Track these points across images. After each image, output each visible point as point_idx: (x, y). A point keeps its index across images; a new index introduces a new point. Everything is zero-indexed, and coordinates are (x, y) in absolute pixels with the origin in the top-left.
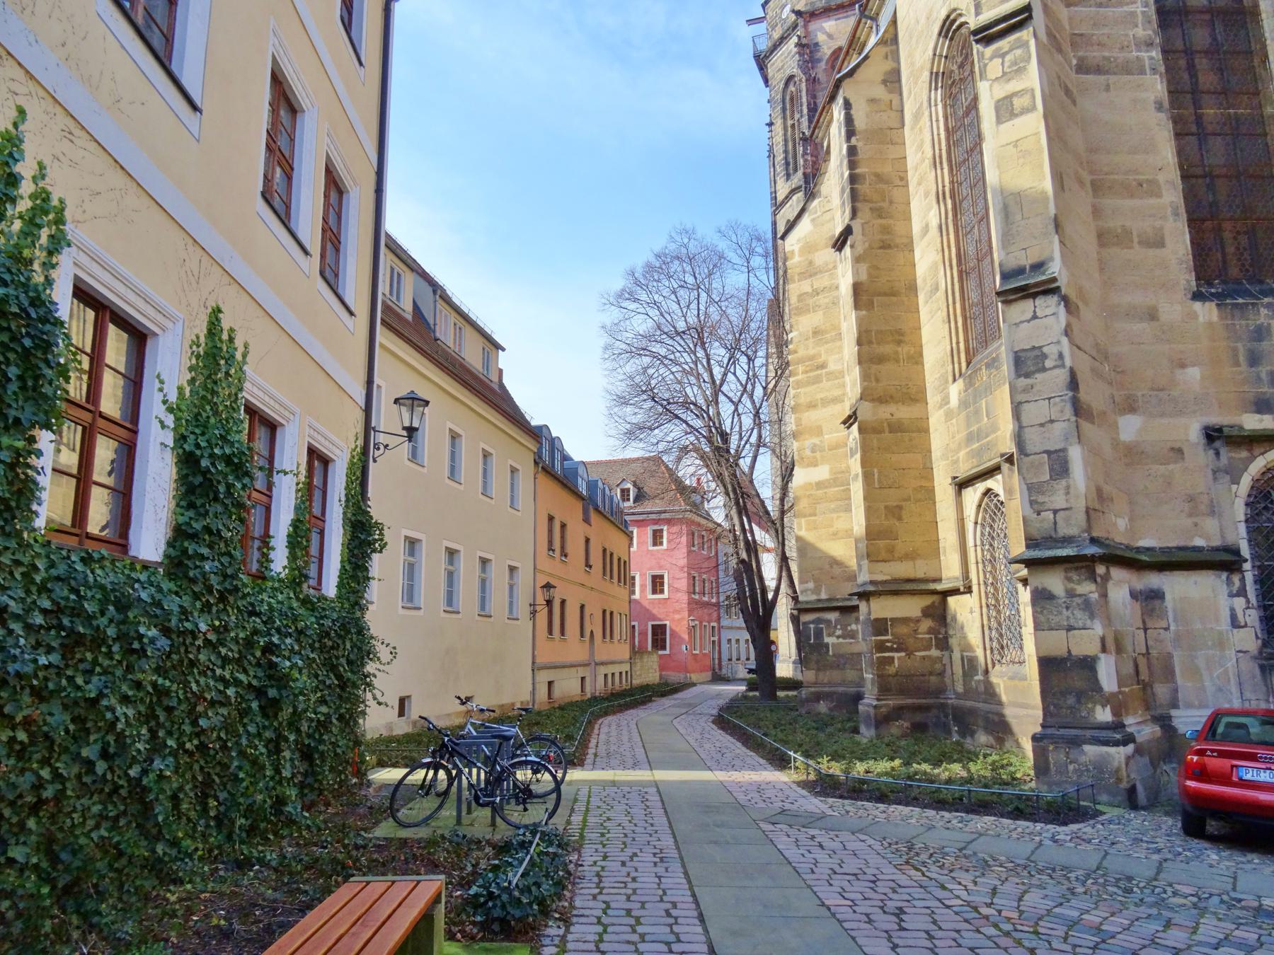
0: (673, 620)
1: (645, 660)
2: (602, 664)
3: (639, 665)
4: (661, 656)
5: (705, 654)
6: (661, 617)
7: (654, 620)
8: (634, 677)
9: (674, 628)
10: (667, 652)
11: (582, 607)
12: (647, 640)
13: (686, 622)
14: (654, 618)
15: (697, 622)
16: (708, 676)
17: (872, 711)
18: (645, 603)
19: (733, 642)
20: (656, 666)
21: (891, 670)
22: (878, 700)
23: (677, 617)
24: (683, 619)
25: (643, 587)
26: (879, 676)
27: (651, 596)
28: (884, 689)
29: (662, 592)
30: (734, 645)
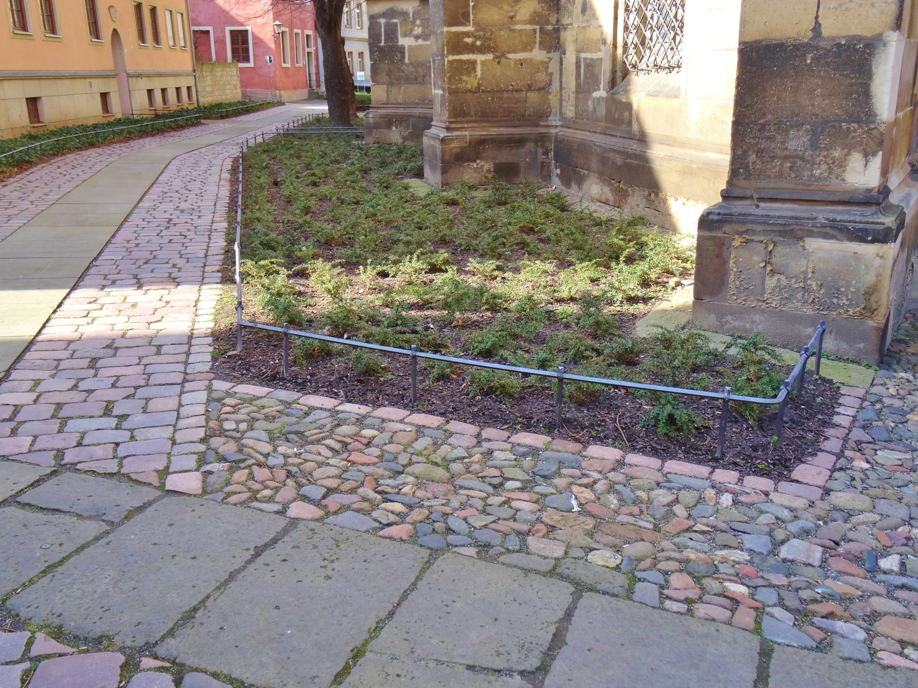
0: (255, 25)
1: (218, 74)
2: (139, 76)
4: (242, 70)
6: (241, 20)
7: (232, 25)
9: (257, 33)
10: (251, 64)
12: (225, 49)
13: (270, 28)
14: (232, 20)
16: (303, 93)
17: (438, 145)
20: (236, 81)
21: (470, 82)
22: (448, 129)
26: (452, 92)
28: (458, 114)
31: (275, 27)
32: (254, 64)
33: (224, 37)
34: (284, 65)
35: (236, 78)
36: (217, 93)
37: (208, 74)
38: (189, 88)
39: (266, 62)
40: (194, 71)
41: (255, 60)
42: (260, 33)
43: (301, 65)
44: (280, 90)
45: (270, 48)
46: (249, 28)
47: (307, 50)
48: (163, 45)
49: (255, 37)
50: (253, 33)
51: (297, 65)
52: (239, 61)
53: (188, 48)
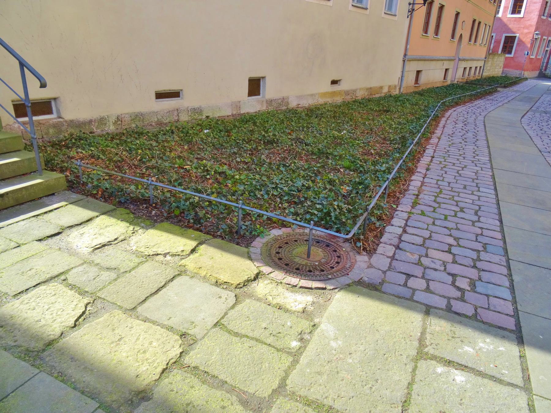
0: (522, 33)
1: (495, 60)
2: (464, 60)
3: (490, 62)
6: (514, 30)
7: (508, 33)
8: (485, 71)
9: (521, 38)
10: (512, 55)
11: (457, 14)
13: (531, 36)
14: (509, 30)
15: (540, 36)
18: (505, 20)
20: (502, 65)
23: (526, 31)
24: (529, 33)
25: (506, 8)
27: (510, 16)
29: (519, 12)
31: (535, 35)
33: (501, 39)
34: (531, 57)
36: (491, 71)
37: (491, 60)
38: (481, 67)
39: (525, 55)
40: (486, 58)
41: (515, 53)
42: (524, 38)
43: (540, 57)
44: (524, 70)
45: (527, 47)
46: (518, 35)
48: (478, 44)
49: (520, 41)
50: (519, 38)
51: (538, 57)
52: (506, 53)
53: (487, 46)
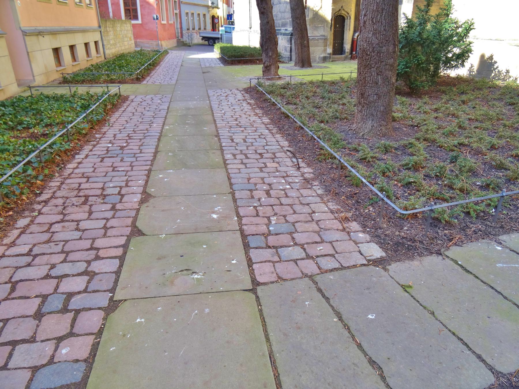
1: (118, 29)
2: (40, 33)
3: (111, 33)
4: (134, 26)
5: (171, 24)
8: (106, 47)
10: (139, 22)
19: (190, 15)
20: (130, 35)
30: (190, 18)
32: (142, 21)
34: (163, 22)
35: (130, 32)
36: (118, 45)
37: (111, 29)
38: (96, 43)
40: (100, 27)
44: (161, 40)
47: (175, 11)
51: (170, 22)
53: (93, 6)
